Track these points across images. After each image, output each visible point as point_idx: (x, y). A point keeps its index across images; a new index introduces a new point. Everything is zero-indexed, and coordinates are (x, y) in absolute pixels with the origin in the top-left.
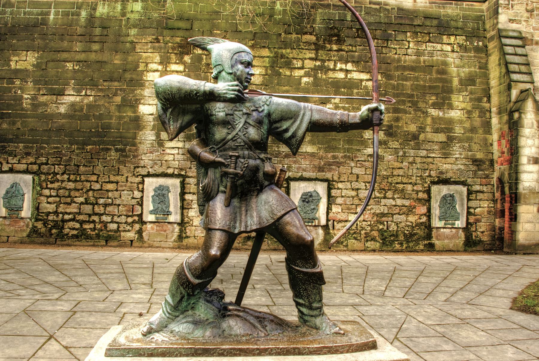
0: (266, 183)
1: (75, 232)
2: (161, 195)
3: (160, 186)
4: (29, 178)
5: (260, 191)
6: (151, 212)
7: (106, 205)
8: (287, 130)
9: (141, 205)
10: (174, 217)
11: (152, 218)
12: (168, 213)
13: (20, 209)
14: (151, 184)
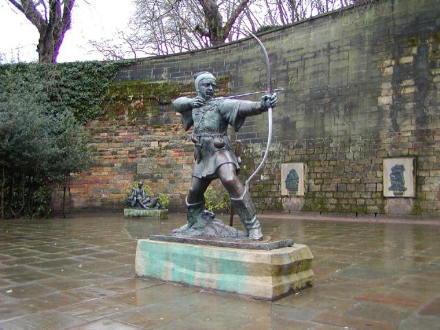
0: (217, 149)
1: (334, 207)
2: (398, 172)
3: (396, 166)
4: (301, 165)
5: (213, 153)
6: (391, 189)
7: (356, 183)
8: (229, 117)
9: (382, 183)
10: (410, 191)
11: (391, 194)
12: (405, 190)
13: (296, 189)
14: (389, 164)
